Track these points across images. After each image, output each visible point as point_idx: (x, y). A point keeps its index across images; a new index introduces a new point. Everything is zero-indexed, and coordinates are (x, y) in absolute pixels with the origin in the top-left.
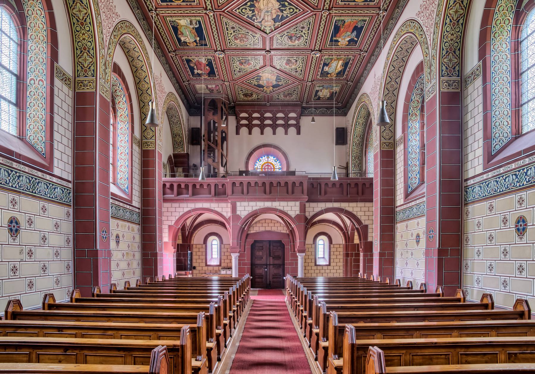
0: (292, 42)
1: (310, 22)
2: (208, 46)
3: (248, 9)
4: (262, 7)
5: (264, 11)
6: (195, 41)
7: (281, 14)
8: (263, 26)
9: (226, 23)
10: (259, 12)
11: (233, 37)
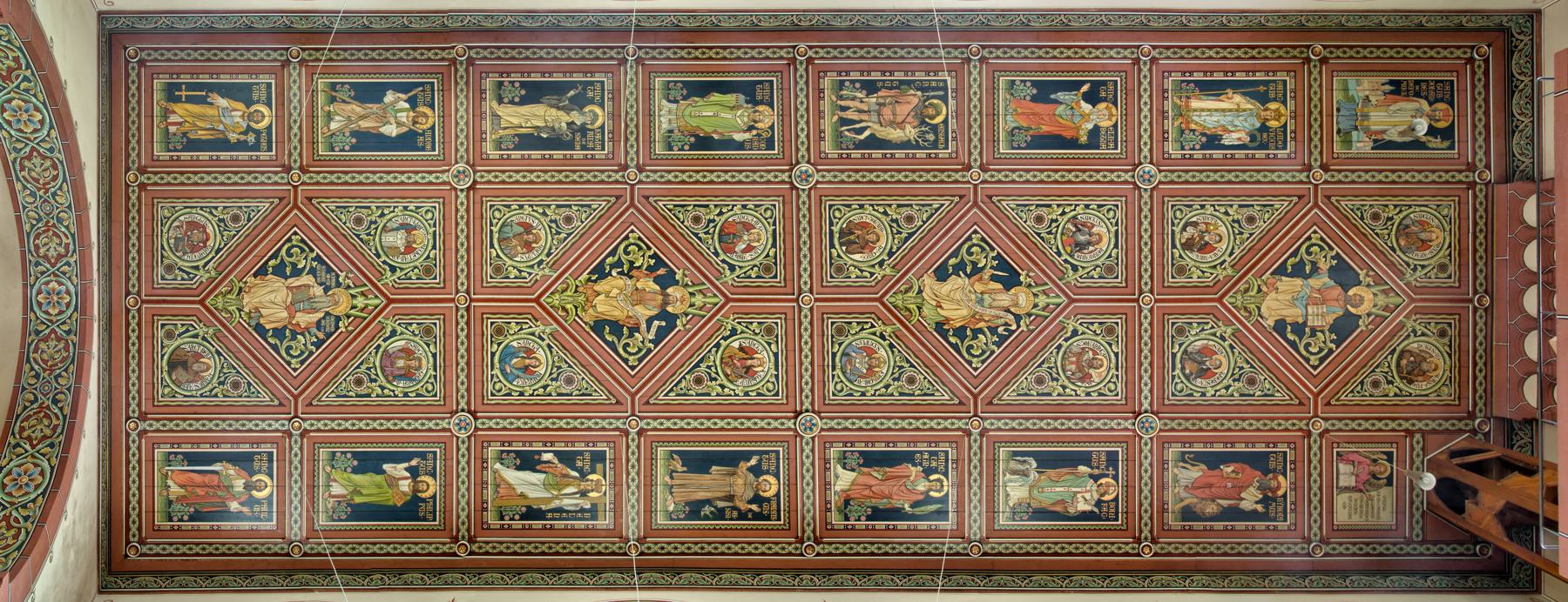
0: (1100, 240)
1: (1018, 205)
2: (1120, 449)
3: (971, 343)
4: (965, 312)
5: (978, 309)
6: (1095, 478)
7: (987, 273)
8: (1034, 311)
9: (1018, 395)
10: (981, 320)
11: (1079, 384)
